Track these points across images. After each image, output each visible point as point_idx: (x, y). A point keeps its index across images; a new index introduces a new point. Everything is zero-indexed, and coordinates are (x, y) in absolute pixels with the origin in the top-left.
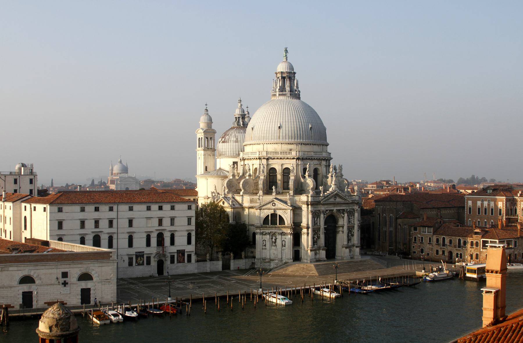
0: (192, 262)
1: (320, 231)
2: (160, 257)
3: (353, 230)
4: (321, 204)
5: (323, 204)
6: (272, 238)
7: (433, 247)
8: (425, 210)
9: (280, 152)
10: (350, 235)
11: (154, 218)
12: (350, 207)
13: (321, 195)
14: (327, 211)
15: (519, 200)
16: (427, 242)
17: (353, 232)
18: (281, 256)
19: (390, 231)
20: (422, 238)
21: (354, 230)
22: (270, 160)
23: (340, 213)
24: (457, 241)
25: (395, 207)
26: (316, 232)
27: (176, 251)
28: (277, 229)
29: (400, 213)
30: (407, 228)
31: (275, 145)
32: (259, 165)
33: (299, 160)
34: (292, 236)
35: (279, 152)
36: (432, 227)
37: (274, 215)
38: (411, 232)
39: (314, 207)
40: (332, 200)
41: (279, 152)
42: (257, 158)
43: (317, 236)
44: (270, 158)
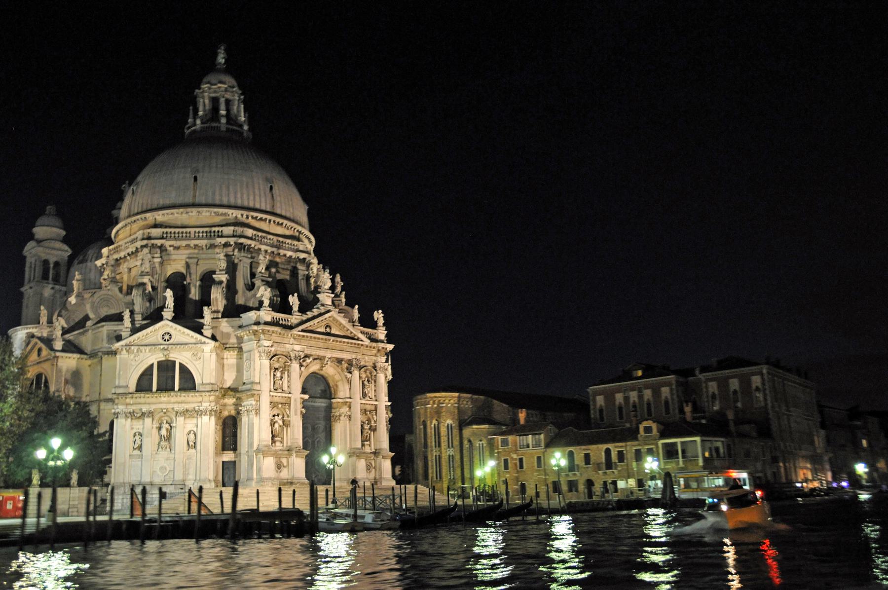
5: (299, 336)
6: (160, 428)
7: (547, 477)
9: (195, 232)
10: (366, 427)
15: (703, 379)
17: (375, 422)
19: (449, 456)
20: (521, 460)
21: (376, 415)
23: (342, 371)
24: (603, 454)
26: (280, 406)
30: (485, 445)
34: (213, 418)
37: (166, 367)
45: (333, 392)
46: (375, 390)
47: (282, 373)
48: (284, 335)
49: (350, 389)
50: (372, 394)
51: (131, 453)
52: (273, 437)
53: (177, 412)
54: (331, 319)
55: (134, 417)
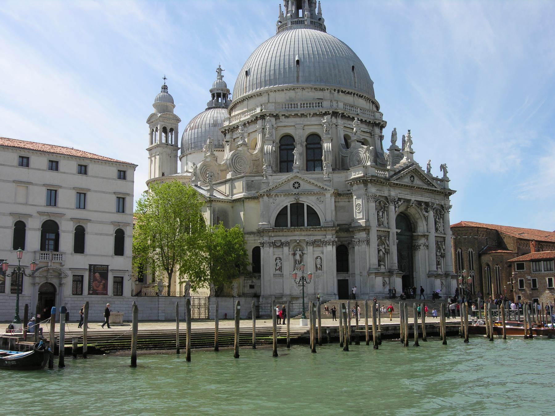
0: (124, 295)
1: (389, 238)
2: (46, 278)
3: (444, 246)
4: (391, 186)
5: (394, 184)
6: (294, 254)
8: (522, 242)
9: (301, 104)
10: (438, 254)
11: (37, 185)
12: (437, 201)
13: (389, 167)
14: (400, 201)
16: (544, 286)
18: (315, 289)
20: (534, 281)
21: (445, 245)
22: (281, 120)
23: (421, 210)
25: (476, 237)
26: (383, 239)
27: (88, 267)
28: (303, 233)
29: (483, 247)
31: (291, 91)
32: (261, 130)
33: (336, 117)
34: (335, 247)
35: (299, 104)
36: (552, 260)
37: (297, 208)
38: (513, 273)
39: (377, 190)
40: (406, 181)
41: (299, 104)
42: (257, 117)
43: (385, 249)
44: (283, 115)
45: (413, 227)
46: (443, 226)
47: (383, 213)
48: (384, 183)
49: (427, 225)
50: (441, 229)
51: (276, 273)
52: (379, 261)
53: (307, 243)
54: (414, 171)
55: (275, 246)
